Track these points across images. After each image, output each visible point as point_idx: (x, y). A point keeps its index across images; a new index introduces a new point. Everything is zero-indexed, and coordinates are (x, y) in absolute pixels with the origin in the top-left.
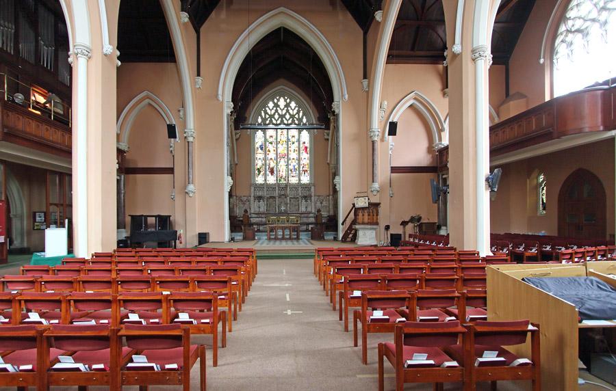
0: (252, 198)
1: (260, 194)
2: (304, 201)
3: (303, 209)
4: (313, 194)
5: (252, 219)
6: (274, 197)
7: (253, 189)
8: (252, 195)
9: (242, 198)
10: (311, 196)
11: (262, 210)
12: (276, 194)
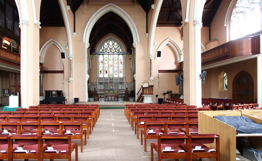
0: (98, 83)
1: (101, 82)
3: (120, 88)
4: (124, 82)
5: (98, 92)
6: (108, 83)
7: (98, 79)
8: (98, 82)
10: (123, 83)
12: (108, 81)
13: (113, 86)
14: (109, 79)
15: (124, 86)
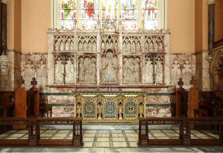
0: (50, 58)
1: (67, 49)
2: (149, 62)
3: (147, 79)
4: (167, 50)
5: (49, 97)
6: (93, 56)
7: (52, 38)
8: (51, 50)
9: (32, 58)
10: (163, 54)
11: (71, 78)
12: (97, 48)
13: (117, 69)
14: (103, 36)
15: (167, 68)
